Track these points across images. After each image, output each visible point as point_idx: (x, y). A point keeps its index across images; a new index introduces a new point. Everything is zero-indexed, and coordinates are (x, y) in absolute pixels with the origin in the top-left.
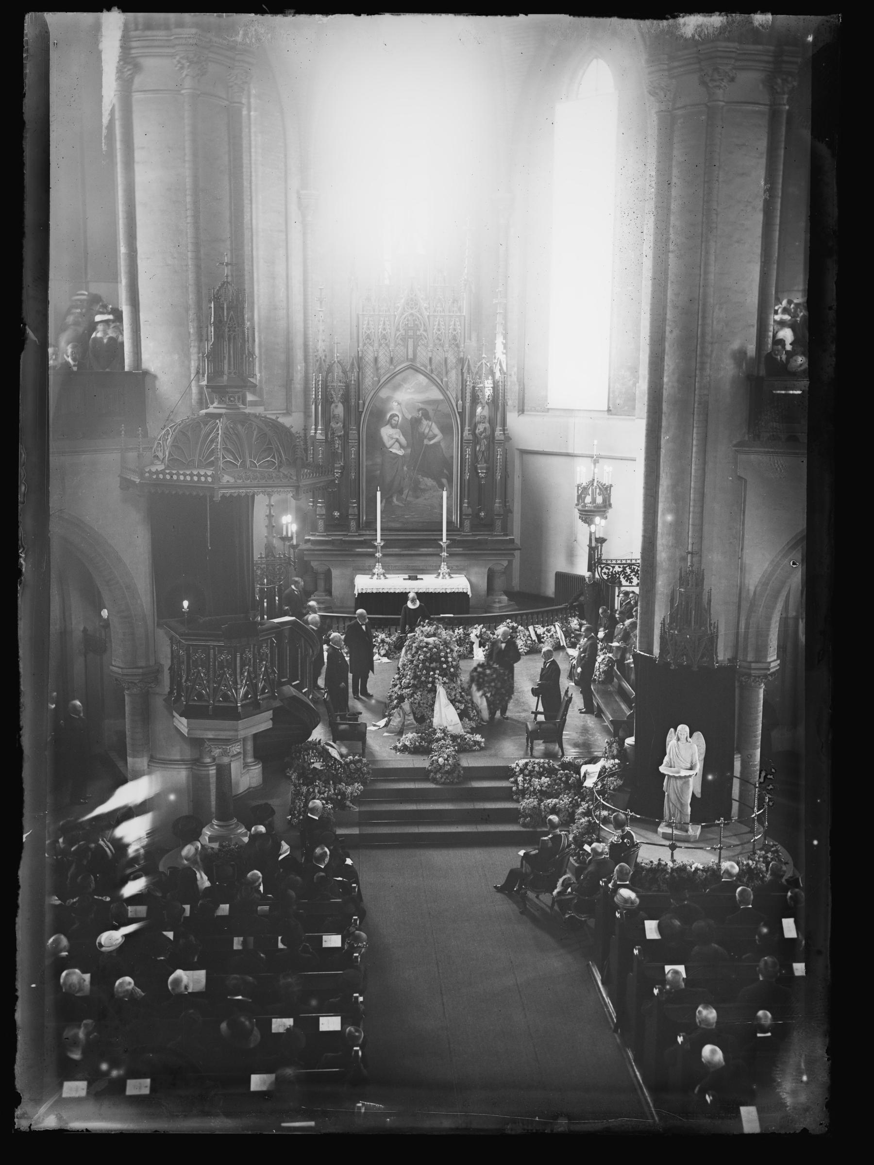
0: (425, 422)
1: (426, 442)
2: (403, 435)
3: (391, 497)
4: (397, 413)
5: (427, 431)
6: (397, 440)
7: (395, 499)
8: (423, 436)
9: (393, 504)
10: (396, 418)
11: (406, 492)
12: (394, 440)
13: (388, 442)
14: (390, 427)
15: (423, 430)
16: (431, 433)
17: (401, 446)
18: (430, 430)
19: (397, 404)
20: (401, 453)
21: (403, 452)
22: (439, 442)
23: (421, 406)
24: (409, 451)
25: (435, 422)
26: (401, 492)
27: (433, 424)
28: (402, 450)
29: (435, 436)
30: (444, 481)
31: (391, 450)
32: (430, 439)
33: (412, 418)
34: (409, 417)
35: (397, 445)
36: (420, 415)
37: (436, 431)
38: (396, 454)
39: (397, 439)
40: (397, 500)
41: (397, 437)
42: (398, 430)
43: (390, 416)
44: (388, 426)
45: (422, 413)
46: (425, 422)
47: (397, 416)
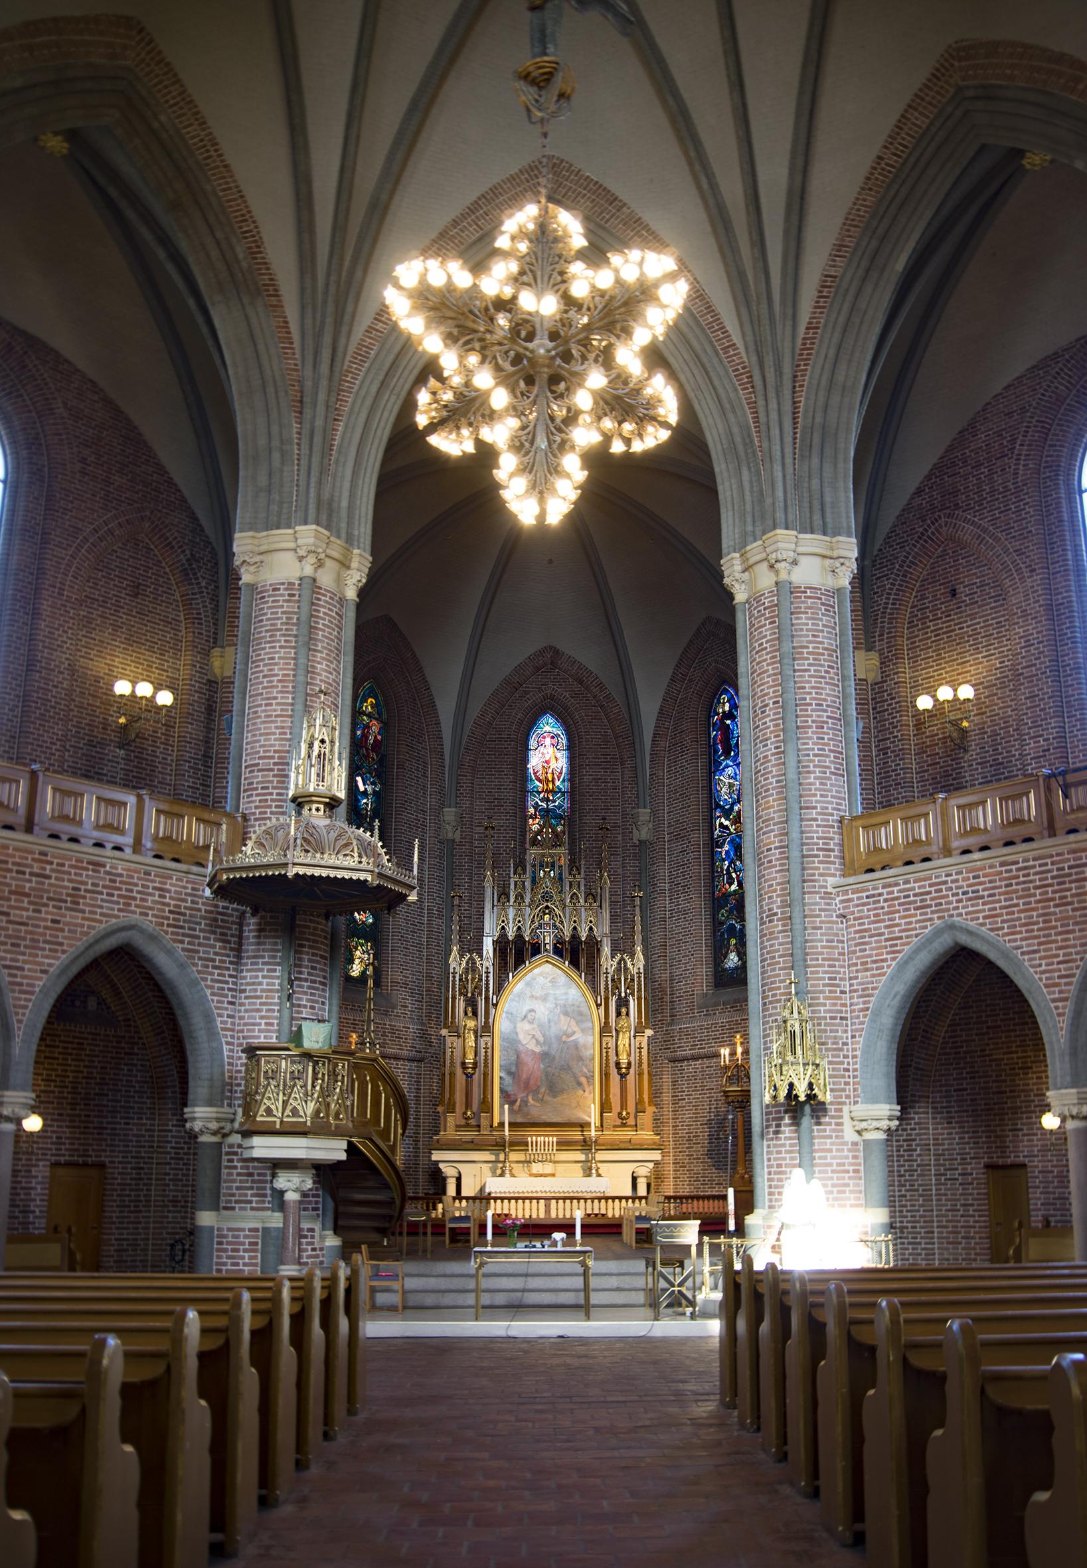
11: (543, 1090)
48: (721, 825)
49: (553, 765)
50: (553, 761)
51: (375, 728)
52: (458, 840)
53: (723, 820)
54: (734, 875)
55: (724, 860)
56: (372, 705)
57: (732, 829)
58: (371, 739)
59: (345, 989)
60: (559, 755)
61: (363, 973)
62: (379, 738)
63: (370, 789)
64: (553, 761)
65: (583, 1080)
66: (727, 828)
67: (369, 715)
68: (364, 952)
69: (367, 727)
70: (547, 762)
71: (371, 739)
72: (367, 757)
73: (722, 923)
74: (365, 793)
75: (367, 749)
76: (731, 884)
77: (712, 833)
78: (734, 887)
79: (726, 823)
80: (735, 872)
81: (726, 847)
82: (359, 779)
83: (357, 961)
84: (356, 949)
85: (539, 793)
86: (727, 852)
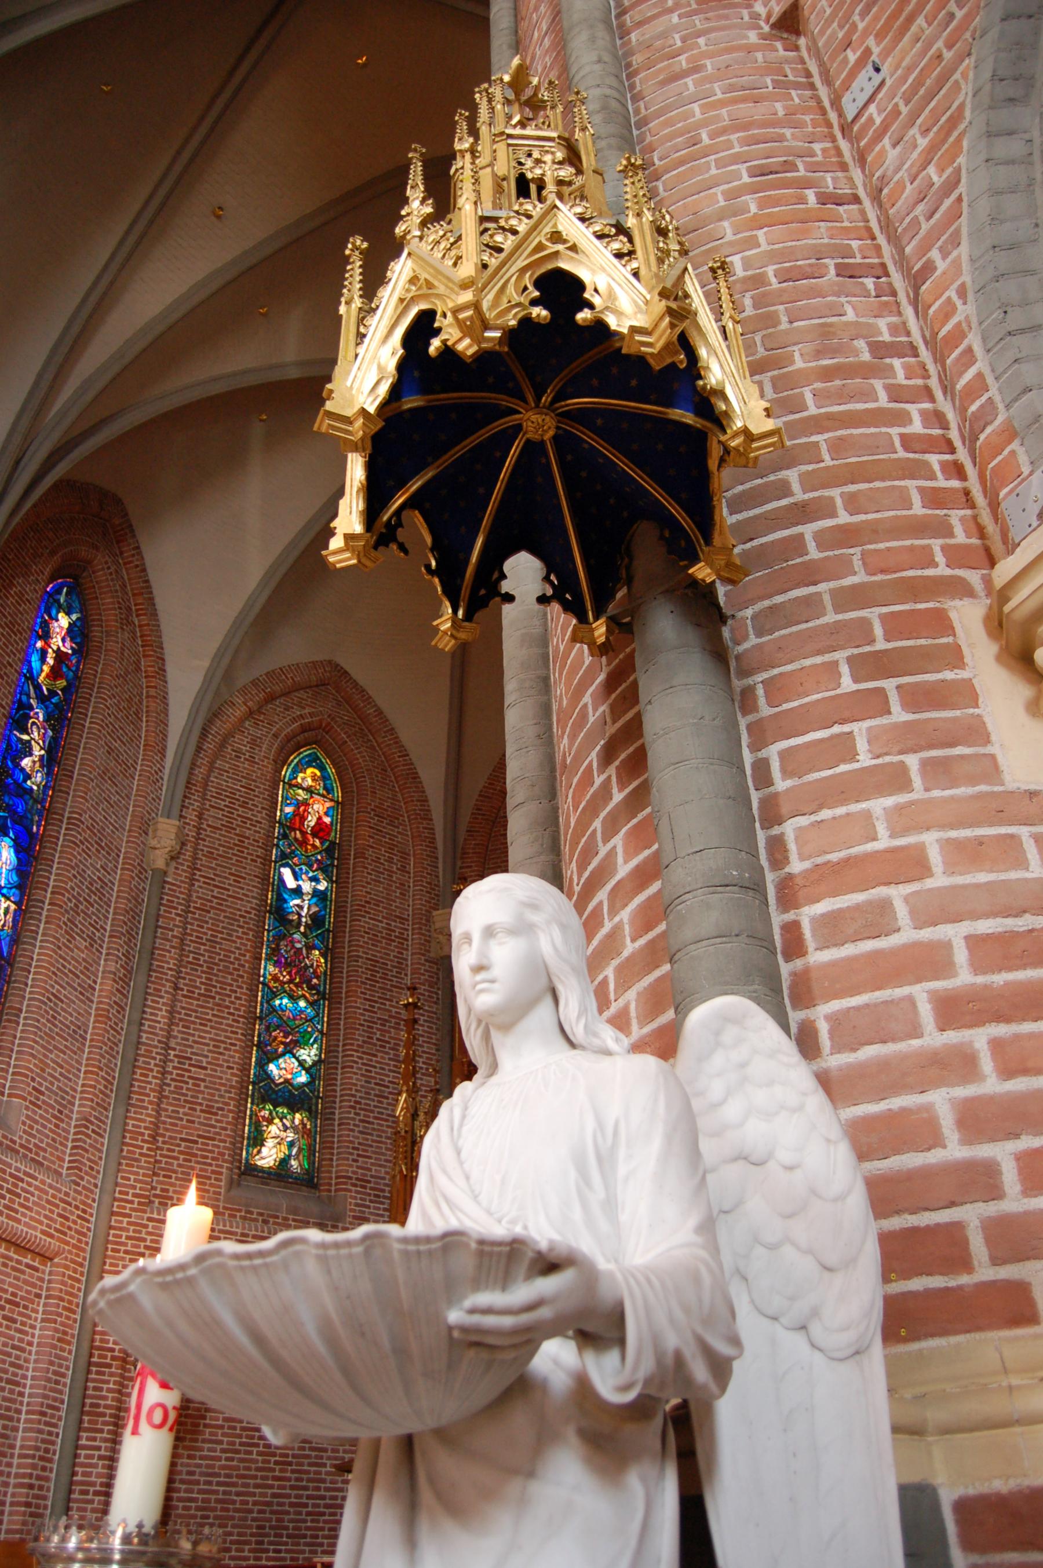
51: (319, 809)
56: (314, 778)
58: (311, 821)
59: (231, 1184)
61: (284, 1162)
62: (327, 820)
63: (307, 887)
67: (308, 790)
68: (286, 1128)
69: (306, 803)
71: (311, 821)
72: (303, 843)
74: (298, 892)
75: (304, 833)
82: (287, 873)
83: (270, 1143)
84: (270, 1121)
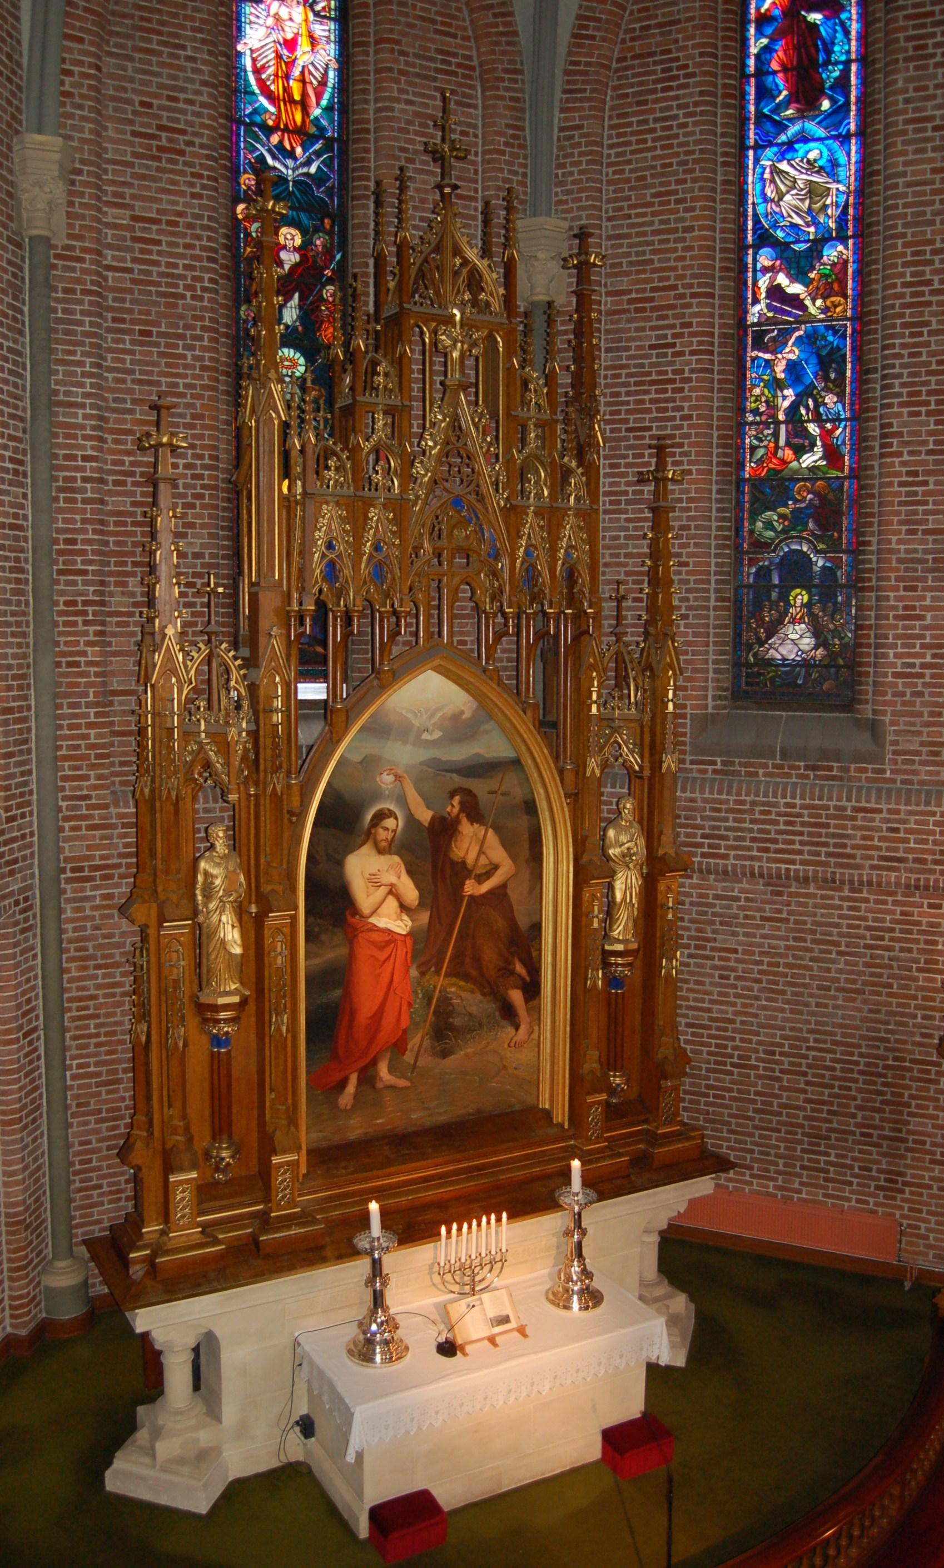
0: (467, 829)
1: (470, 888)
2: (410, 873)
3: (374, 1062)
4: (392, 807)
5: (470, 859)
6: (393, 891)
7: (383, 1070)
8: (461, 871)
9: (379, 1085)
10: (390, 823)
11: (414, 1042)
12: (383, 890)
13: (364, 897)
14: (373, 852)
15: (461, 854)
16: (483, 861)
17: (403, 907)
18: (481, 852)
19: (391, 778)
20: (401, 926)
21: (410, 923)
22: (503, 887)
23: (457, 780)
24: (425, 917)
25: (498, 829)
26: (399, 1046)
27: (491, 831)
28: (405, 917)
29: (496, 867)
30: (516, 996)
31: (373, 920)
32: (481, 879)
33: (433, 818)
34: (425, 816)
35: (392, 903)
36: (456, 810)
37: (497, 853)
38: (389, 932)
39: (392, 885)
40: (390, 1072)
41: (393, 879)
42: (396, 859)
43: (375, 816)
44: (367, 850)
45: (461, 803)
46: (467, 829)
47: (391, 814)
48: (776, 292)
49: (303, 55)
50: (304, 44)
52: (61, 240)
53: (782, 279)
54: (813, 428)
55: (778, 385)
57: (814, 308)
60: (319, 30)
64: (304, 44)
65: (516, 996)
66: (795, 301)
70: (291, 45)
73: (760, 545)
76: (801, 446)
77: (743, 312)
78: (808, 460)
79: (796, 288)
80: (818, 419)
81: (792, 352)
85: (270, 131)
86: (793, 367)
